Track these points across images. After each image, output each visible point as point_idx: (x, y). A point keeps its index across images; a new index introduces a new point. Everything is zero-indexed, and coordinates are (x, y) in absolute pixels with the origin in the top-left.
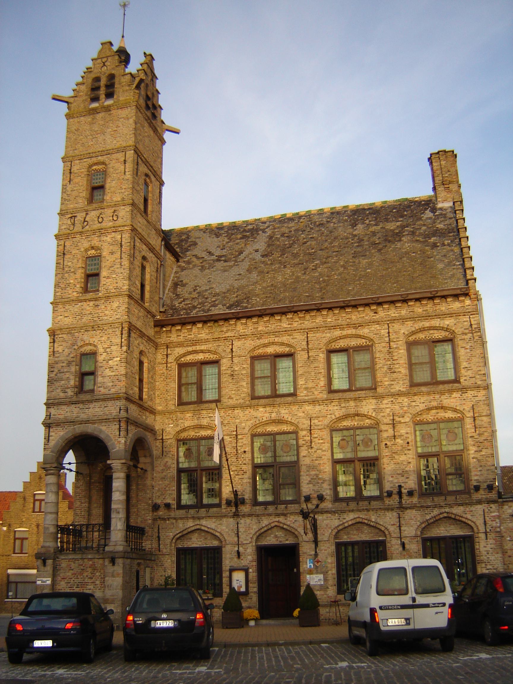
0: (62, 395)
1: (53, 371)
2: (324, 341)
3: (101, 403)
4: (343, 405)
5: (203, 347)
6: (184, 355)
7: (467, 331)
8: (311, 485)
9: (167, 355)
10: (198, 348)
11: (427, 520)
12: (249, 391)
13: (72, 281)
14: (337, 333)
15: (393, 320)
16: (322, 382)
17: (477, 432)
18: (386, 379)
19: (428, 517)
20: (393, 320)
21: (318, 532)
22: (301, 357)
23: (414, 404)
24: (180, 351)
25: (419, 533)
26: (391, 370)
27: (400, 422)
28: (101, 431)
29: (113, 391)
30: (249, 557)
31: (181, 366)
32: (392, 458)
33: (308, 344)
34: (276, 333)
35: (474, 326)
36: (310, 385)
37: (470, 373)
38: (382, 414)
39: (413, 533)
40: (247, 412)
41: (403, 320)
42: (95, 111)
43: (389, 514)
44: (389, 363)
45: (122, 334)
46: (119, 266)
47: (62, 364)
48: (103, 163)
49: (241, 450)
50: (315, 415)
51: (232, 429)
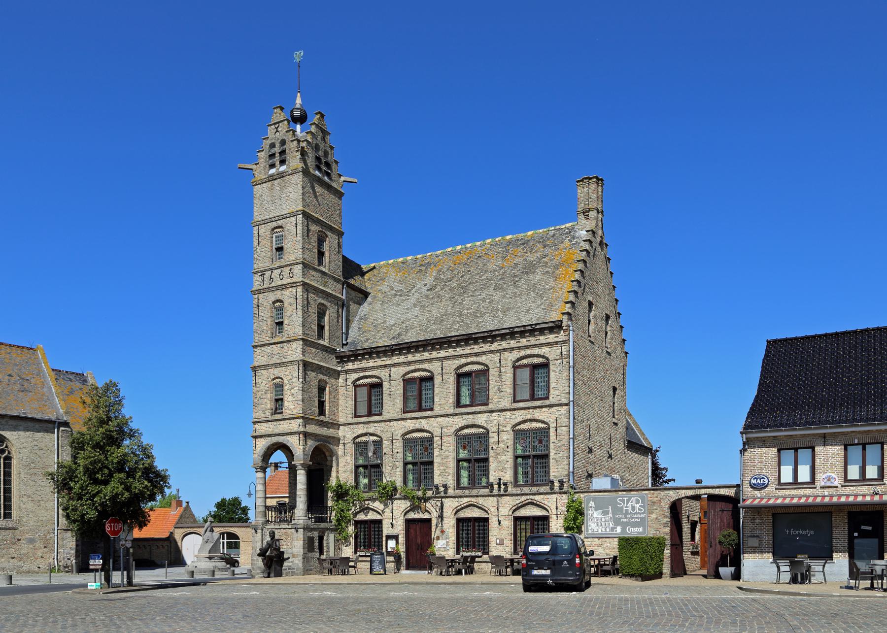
14: (463, 361)
15: (504, 350)
16: (452, 399)
20: (504, 350)
22: (437, 380)
26: (500, 390)
29: (295, 412)
30: (400, 529)
32: (496, 458)
36: (443, 402)
42: (272, 178)
43: (491, 499)
48: (281, 227)
49: (395, 452)
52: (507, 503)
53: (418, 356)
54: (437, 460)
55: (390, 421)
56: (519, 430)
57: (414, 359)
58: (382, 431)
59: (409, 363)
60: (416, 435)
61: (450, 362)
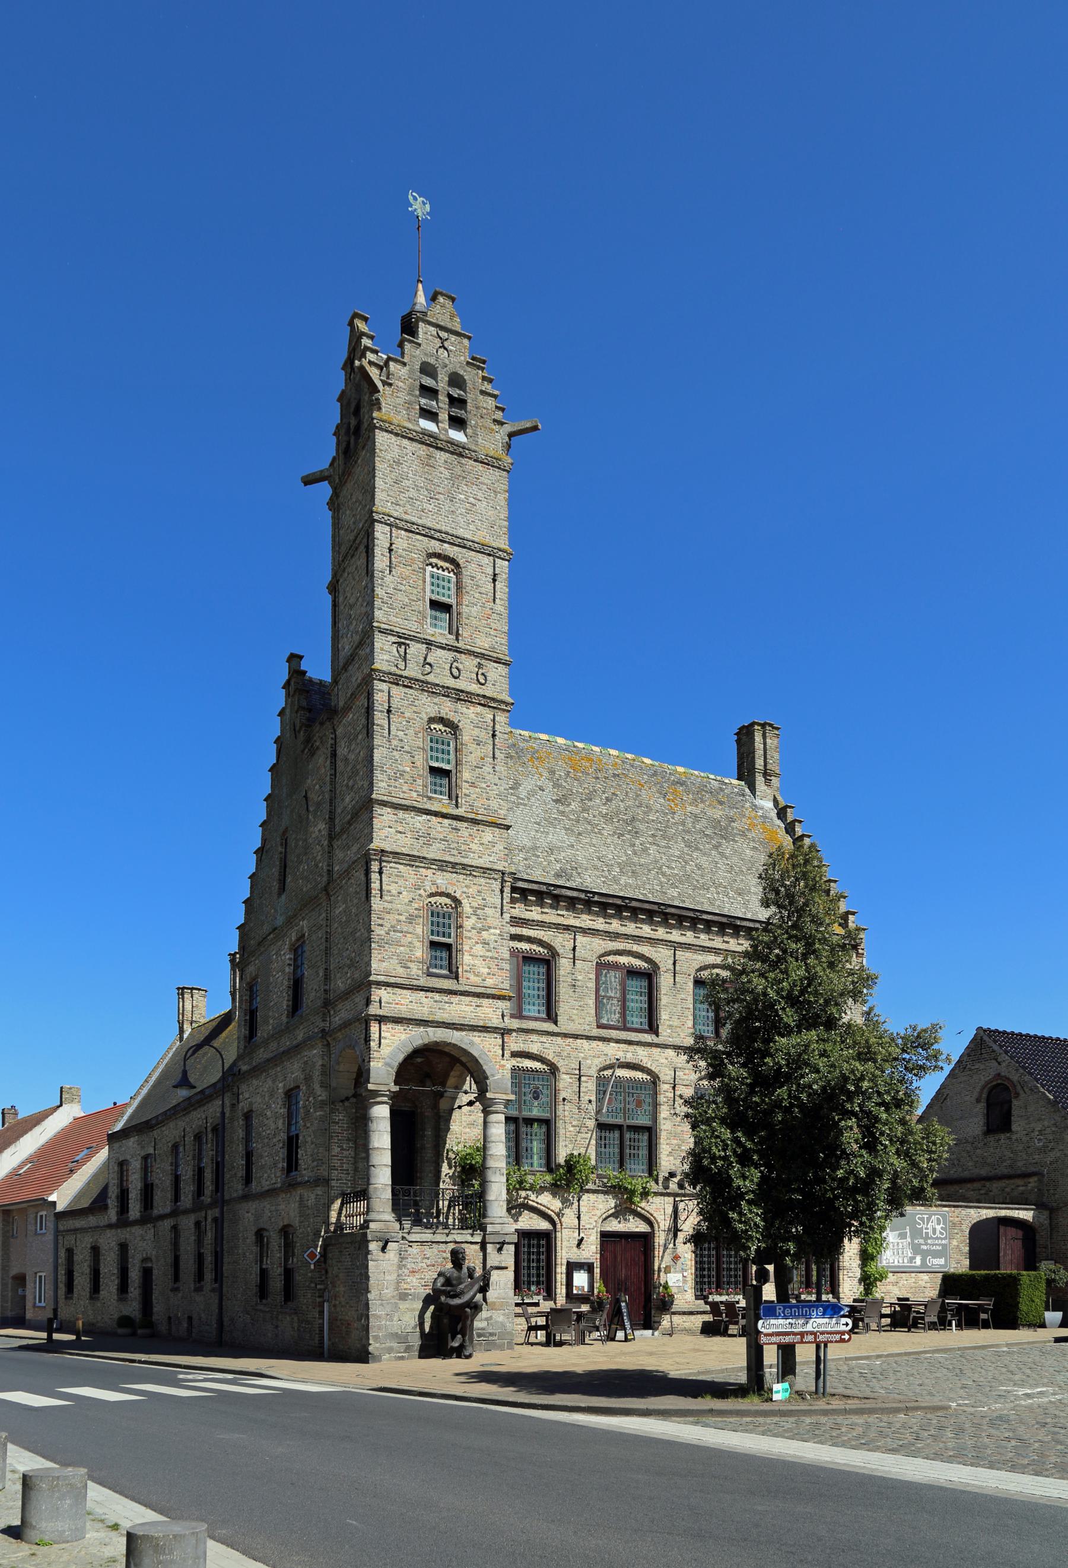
0: (401, 971)
1: (382, 925)
3: (470, 999)
13: (408, 769)
28: (472, 1043)
29: (490, 982)
36: (676, 1023)
45: (502, 892)
46: (491, 771)
47: (397, 917)
51: (573, 1066)
53: (631, 928)
55: (576, 1037)
57: (623, 930)
58: (559, 1055)
59: (616, 936)
60: (621, 1073)
61: (688, 954)
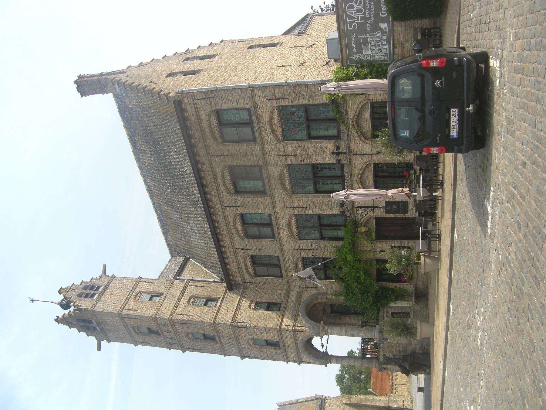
2: (229, 196)
4: (274, 187)
5: (243, 264)
6: (249, 274)
7: (208, 102)
8: (333, 209)
9: (250, 283)
10: (243, 267)
11: (359, 136)
12: (269, 240)
14: (222, 188)
15: (208, 153)
17: (288, 97)
18: (252, 159)
19: (356, 135)
20: (208, 153)
21: (367, 206)
23: (269, 141)
24: (247, 276)
25: (368, 142)
26: (245, 155)
27: (284, 151)
31: (256, 275)
33: (232, 206)
34: (227, 225)
35: (204, 97)
37: (242, 101)
38: (279, 163)
39: (369, 146)
40: (284, 243)
41: (206, 147)
43: (354, 161)
44: (239, 156)
49: (310, 247)
50: (283, 205)
52: (360, 146)
54: (317, 212)
56: (283, 135)
